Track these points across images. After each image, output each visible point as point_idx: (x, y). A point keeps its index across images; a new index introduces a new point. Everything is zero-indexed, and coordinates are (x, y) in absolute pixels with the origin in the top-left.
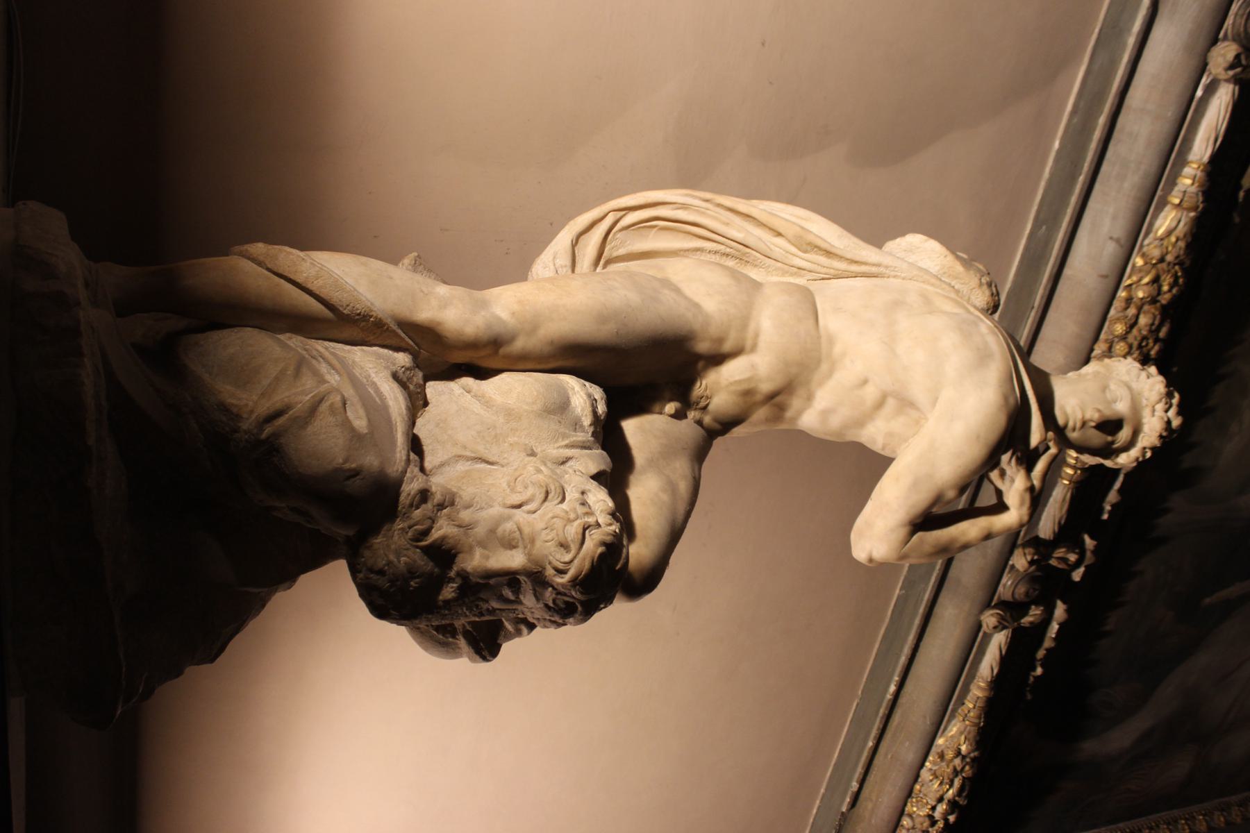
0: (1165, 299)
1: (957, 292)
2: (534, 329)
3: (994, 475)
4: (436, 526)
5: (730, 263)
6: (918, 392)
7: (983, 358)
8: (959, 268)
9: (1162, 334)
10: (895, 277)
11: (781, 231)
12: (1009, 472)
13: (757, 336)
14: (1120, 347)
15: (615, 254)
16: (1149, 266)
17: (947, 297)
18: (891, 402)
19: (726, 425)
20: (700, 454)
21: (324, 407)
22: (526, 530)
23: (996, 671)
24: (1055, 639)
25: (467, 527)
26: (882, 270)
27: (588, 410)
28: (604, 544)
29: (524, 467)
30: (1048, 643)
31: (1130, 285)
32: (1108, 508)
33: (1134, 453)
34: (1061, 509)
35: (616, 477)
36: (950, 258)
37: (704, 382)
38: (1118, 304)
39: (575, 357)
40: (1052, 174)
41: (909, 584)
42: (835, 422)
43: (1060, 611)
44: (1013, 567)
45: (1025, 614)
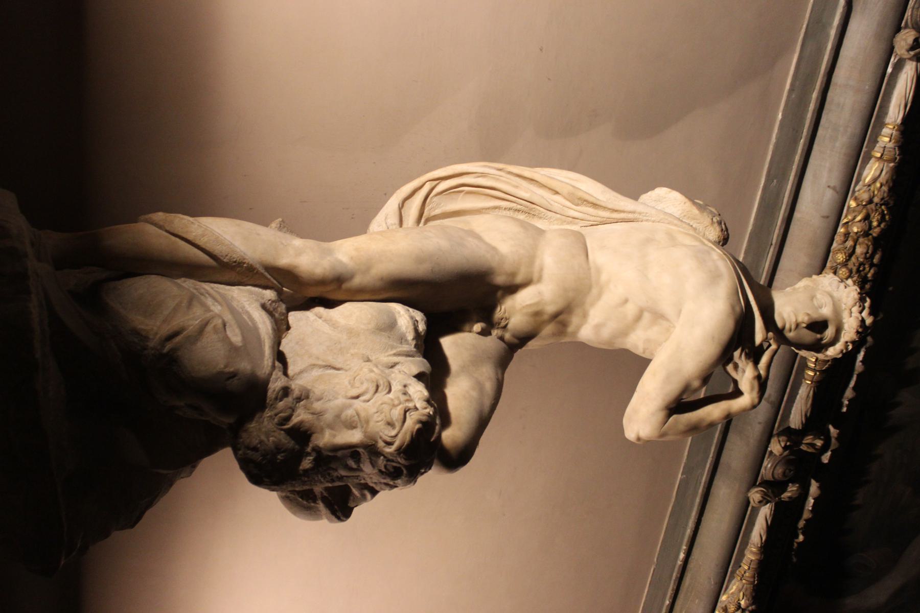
0: (875, 232)
1: (695, 229)
2: (368, 269)
3: (730, 368)
4: (295, 414)
5: (521, 217)
6: (667, 308)
7: (715, 277)
8: (695, 211)
9: (875, 261)
10: (647, 220)
11: (558, 190)
12: (740, 365)
13: (541, 270)
14: (843, 272)
15: (433, 214)
16: (861, 207)
17: (686, 234)
18: (646, 315)
19: (523, 339)
20: (503, 361)
21: (209, 328)
22: (363, 414)
23: (764, 539)
24: (811, 511)
25: (319, 414)
26: (636, 215)
27: (411, 328)
28: (420, 422)
29: (361, 369)
30: (806, 515)
31: (847, 223)
32: (846, 402)
33: (839, 346)
34: (806, 404)
35: (436, 376)
36: (689, 204)
37: (503, 307)
38: (838, 238)
39: (401, 289)
40: (778, 139)
41: (688, 470)
42: (606, 333)
43: (814, 488)
44: (771, 452)
45: (785, 490)
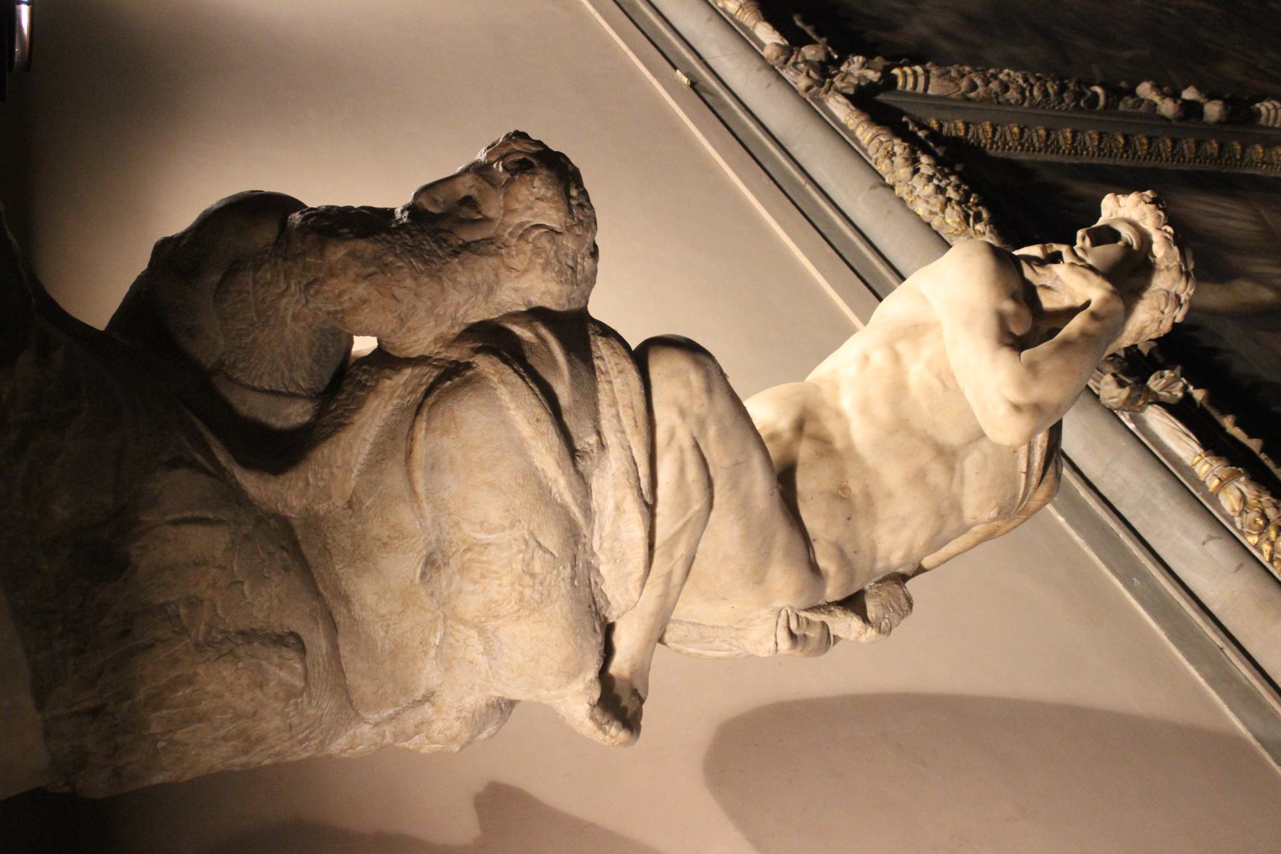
12: (1049, 284)
18: (902, 347)
33: (1157, 237)
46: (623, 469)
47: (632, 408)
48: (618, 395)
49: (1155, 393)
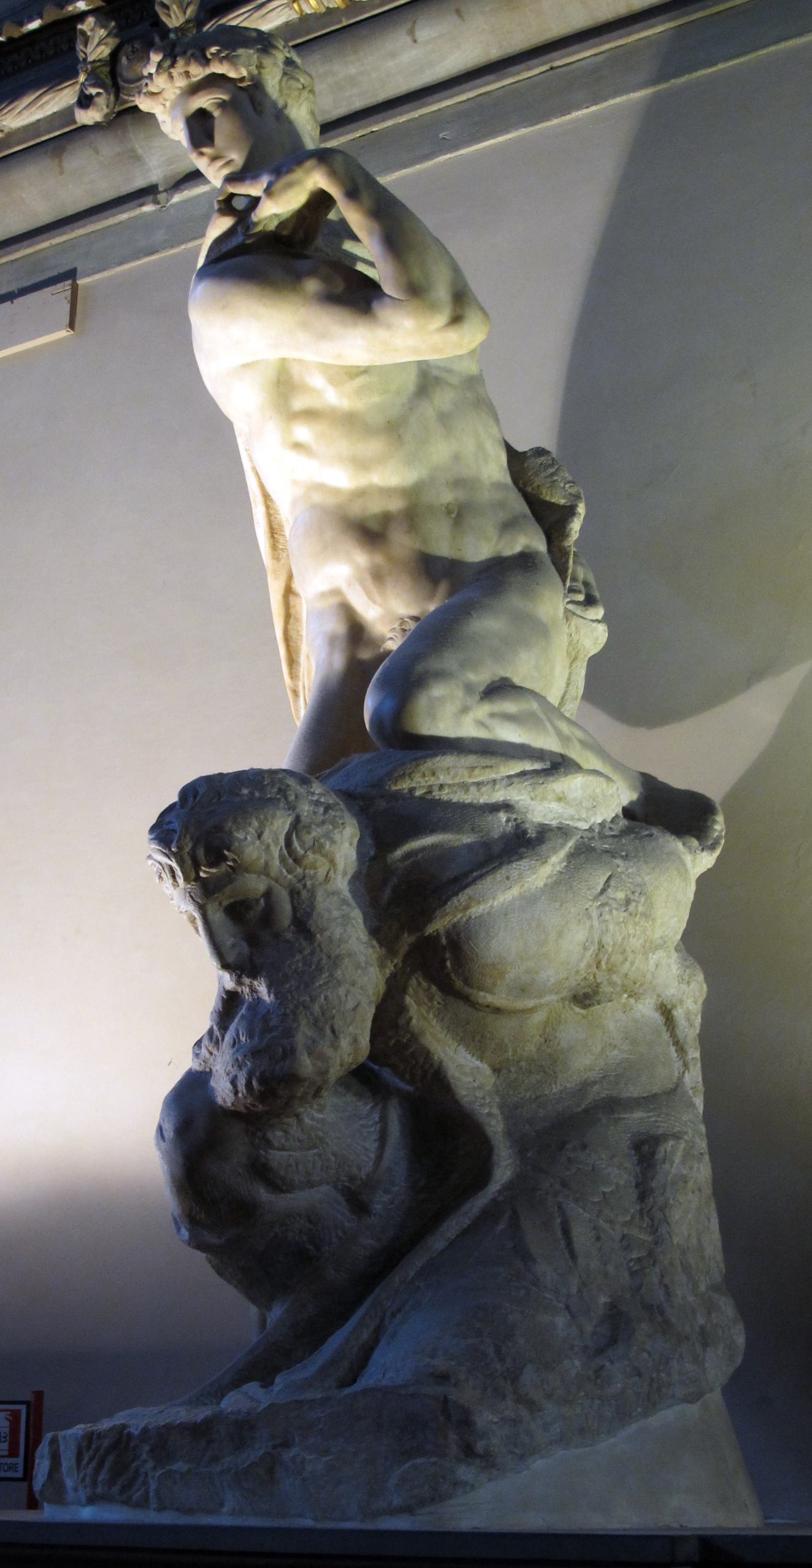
18: (299, 403)
46: (530, 788)
47: (473, 768)
48: (457, 781)
49: (187, 22)
